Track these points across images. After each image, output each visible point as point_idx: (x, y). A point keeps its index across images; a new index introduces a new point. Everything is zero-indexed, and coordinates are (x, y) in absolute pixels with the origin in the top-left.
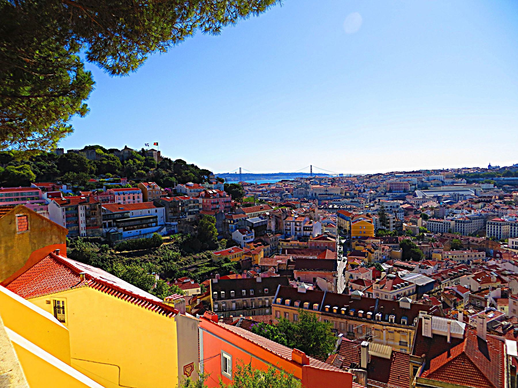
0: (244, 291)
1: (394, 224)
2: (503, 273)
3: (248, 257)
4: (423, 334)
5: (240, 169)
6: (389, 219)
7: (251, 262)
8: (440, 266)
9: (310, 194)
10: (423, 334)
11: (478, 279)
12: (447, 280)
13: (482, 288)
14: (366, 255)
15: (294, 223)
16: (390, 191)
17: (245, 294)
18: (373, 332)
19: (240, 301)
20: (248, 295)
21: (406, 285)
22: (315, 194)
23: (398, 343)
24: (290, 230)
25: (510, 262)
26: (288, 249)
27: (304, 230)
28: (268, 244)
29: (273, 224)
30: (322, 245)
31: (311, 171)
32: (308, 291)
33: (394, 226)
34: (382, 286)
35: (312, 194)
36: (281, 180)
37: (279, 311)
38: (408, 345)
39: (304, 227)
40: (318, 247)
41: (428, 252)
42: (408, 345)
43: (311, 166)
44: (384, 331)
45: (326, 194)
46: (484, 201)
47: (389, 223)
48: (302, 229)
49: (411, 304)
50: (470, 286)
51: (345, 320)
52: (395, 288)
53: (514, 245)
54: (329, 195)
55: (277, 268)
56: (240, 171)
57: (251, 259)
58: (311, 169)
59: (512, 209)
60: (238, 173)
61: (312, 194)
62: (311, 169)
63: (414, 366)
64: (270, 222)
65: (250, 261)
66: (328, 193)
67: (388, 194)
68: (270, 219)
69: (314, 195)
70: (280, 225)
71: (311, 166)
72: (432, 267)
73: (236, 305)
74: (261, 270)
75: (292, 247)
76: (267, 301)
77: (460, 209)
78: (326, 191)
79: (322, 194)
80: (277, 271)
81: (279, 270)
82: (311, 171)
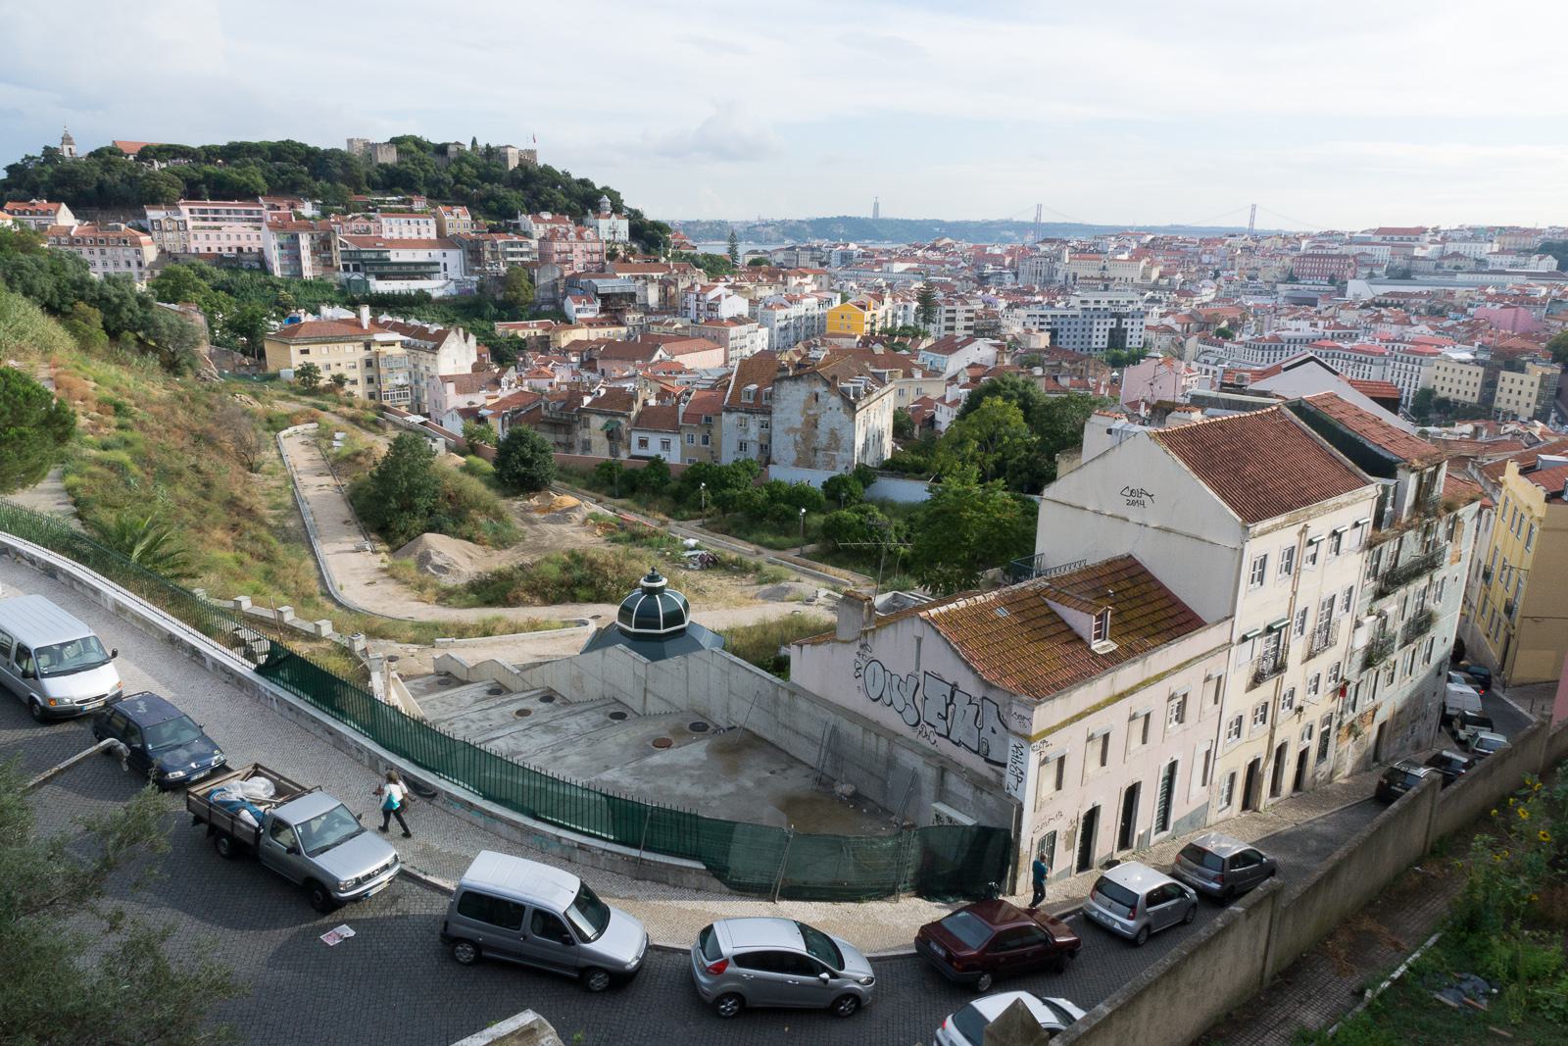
5: (1039, 207)
9: (1060, 277)
16: (1292, 278)
31: (1252, 223)
33: (967, 328)
35: (1067, 277)
43: (1254, 208)
56: (1039, 214)
57: (548, 337)
58: (1253, 217)
60: (1030, 218)
61: (1067, 277)
62: (1253, 217)
66: (1106, 274)
69: (1071, 277)
71: (1254, 208)
78: (1104, 268)
79: (1092, 278)
82: (1252, 223)
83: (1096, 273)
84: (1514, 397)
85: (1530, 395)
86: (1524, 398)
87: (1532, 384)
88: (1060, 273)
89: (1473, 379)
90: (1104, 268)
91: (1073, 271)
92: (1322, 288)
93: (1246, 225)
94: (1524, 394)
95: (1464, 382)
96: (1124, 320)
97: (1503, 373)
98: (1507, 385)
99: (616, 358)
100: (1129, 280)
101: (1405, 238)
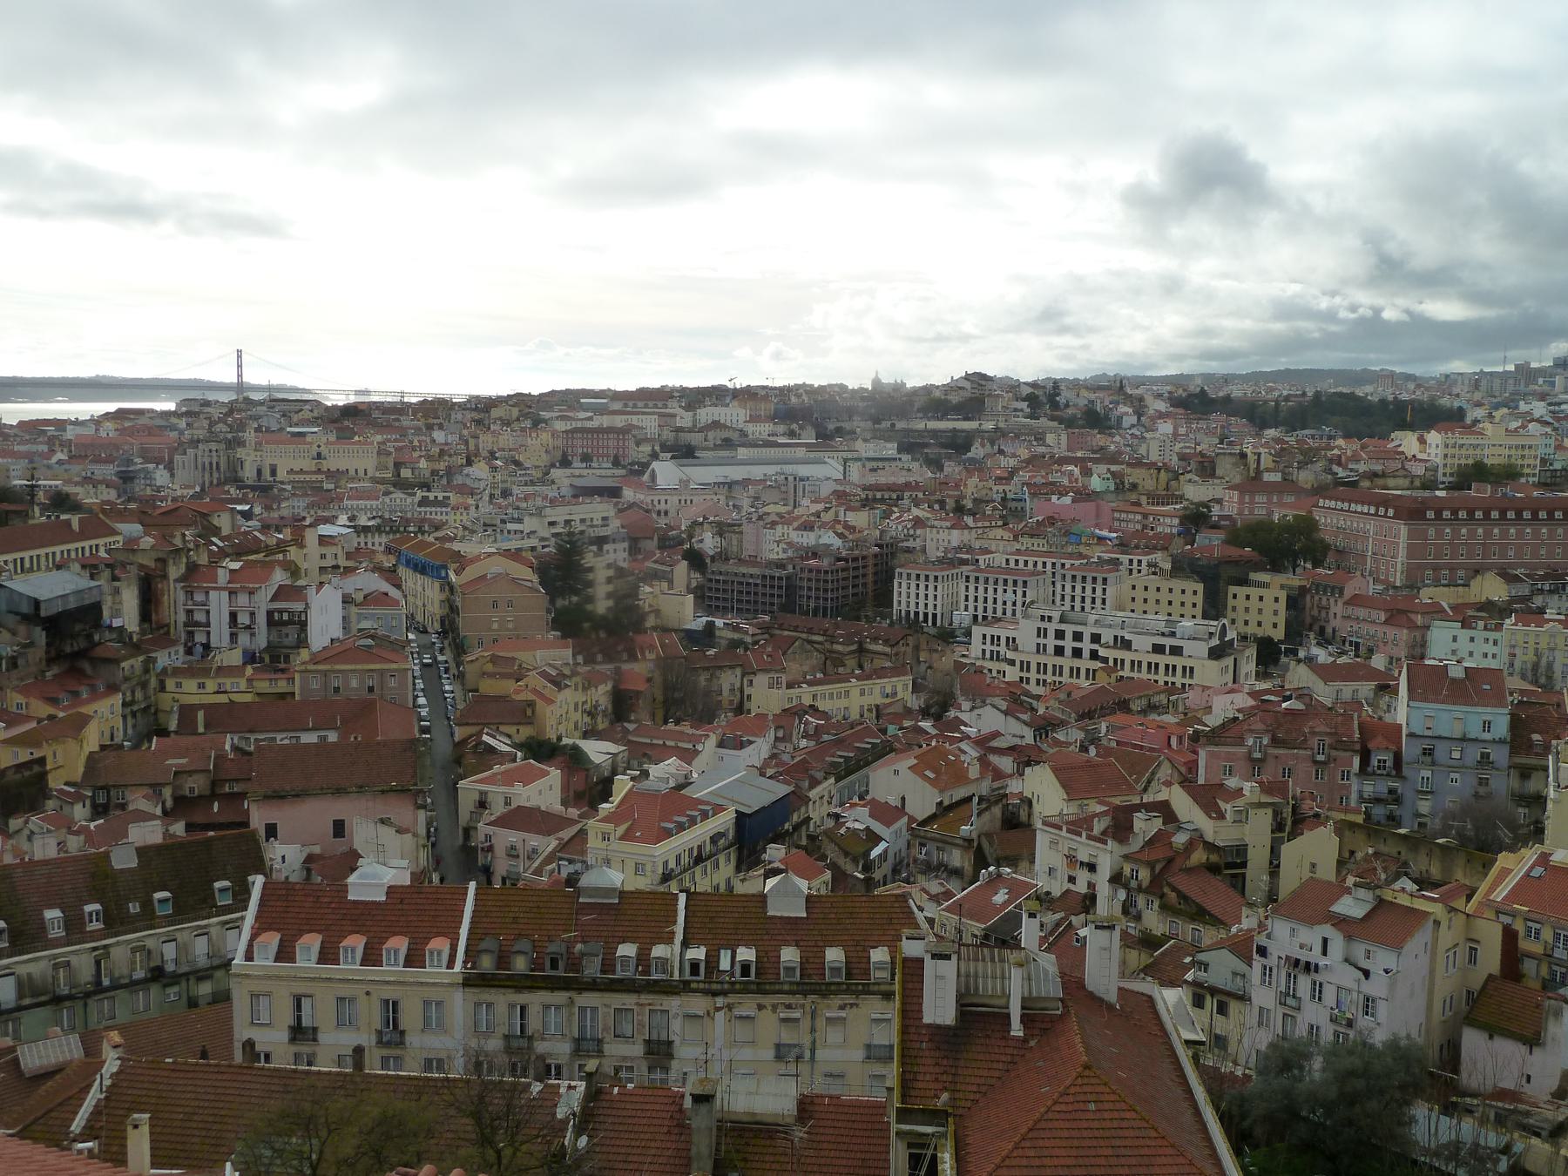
0: (52, 914)
1: (610, 588)
2: (994, 744)
3: (24, 755)
4: (927, 1020)
6: (591, 569)
7: (42, 777)
8: (780, 734)
10: (927, 1020)
11: (928, 773)
12: (825, 784)
13: (946, 803)
14: (529, 712)
15: (225, 595)
16: (565, 463)
17: (56, 932)
18: (676, 1025)
19: (34, 964)
20: (75, 928)
21: (705, 816)
22: (273, 472)
23: (771, 1054)
24: (208, 624)
25: (994, 706)
26: (208, 708)
27: (271, 622)
28: (112, 688)
29: (130, 599)
30: (354, 683)
32: (391, 890)
34: (621, 829)
35: (259, 472)
36: (112, 407)
37: (268, 994)
38: (807, 1054)
39: (270, 614)
40: (337, 690)
41: (738, 685)
42: (807, 1054)
44: (720, 1016)
45: (319, 471)
46: (882, 500)
47: (590, 584)
48: (262, 619)
49: (809, 898)
50: (903, 799)
51: (560, 997)
52: (668, 834)
53: (988, 647)
54: (330, 474)
55: (167, 792)
58: (240, 366)
59: (967, 527)
62: (240, 366)
63: (910, 1146)
64: (117, 591)
65: (36, 769)
66: (325, 465)
67: (556, 473)
68: (115, 578)
70: (158, 603)
72: (760, 741)
73: (20, 985)
74: (94, 806)
75: (223, 699)
76: (169, 951)
77: (812, 529)
78: (319, 456)
80: (169, 804)
81: (179, 800)
83: (308, 464)
84: (1253, 617)
85: (1276, 613)
86: (1268, 619)
87: (1276, 600)
88: (247, 465)
89: (1189, 598)
90: (319, 456)
91: (269, 461)
92: (603, 472)
93: (231, 378)
94: (1268, 612)
95: (1189, 605)
96: (606, 547)
97: (1232, 589)
98: (1241, 603)
99: (361, 789)
100: (361, 473)
101: (651, 404)
